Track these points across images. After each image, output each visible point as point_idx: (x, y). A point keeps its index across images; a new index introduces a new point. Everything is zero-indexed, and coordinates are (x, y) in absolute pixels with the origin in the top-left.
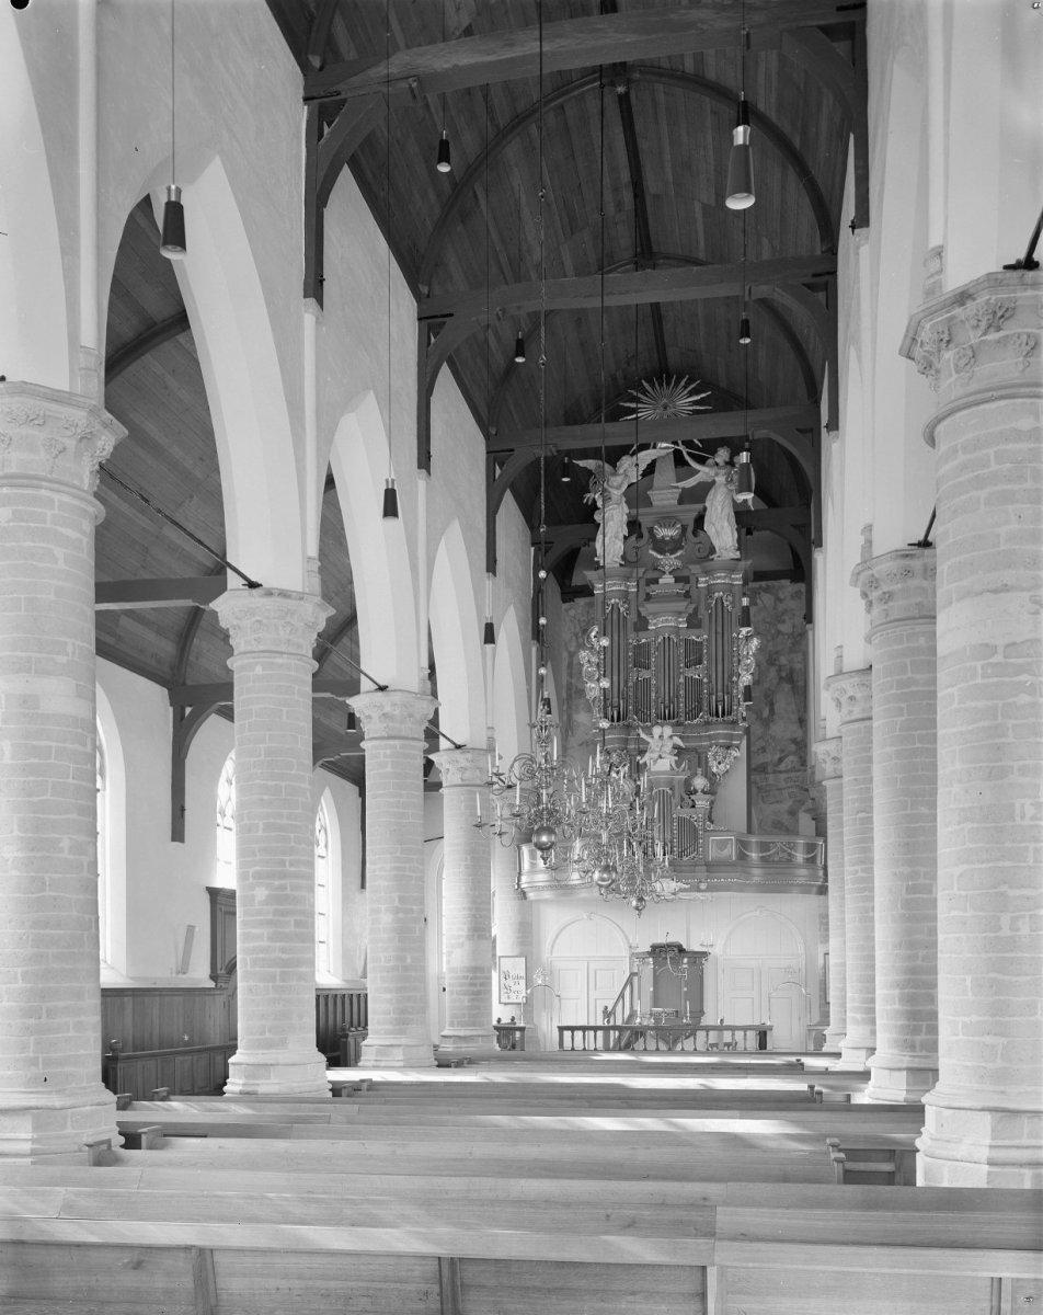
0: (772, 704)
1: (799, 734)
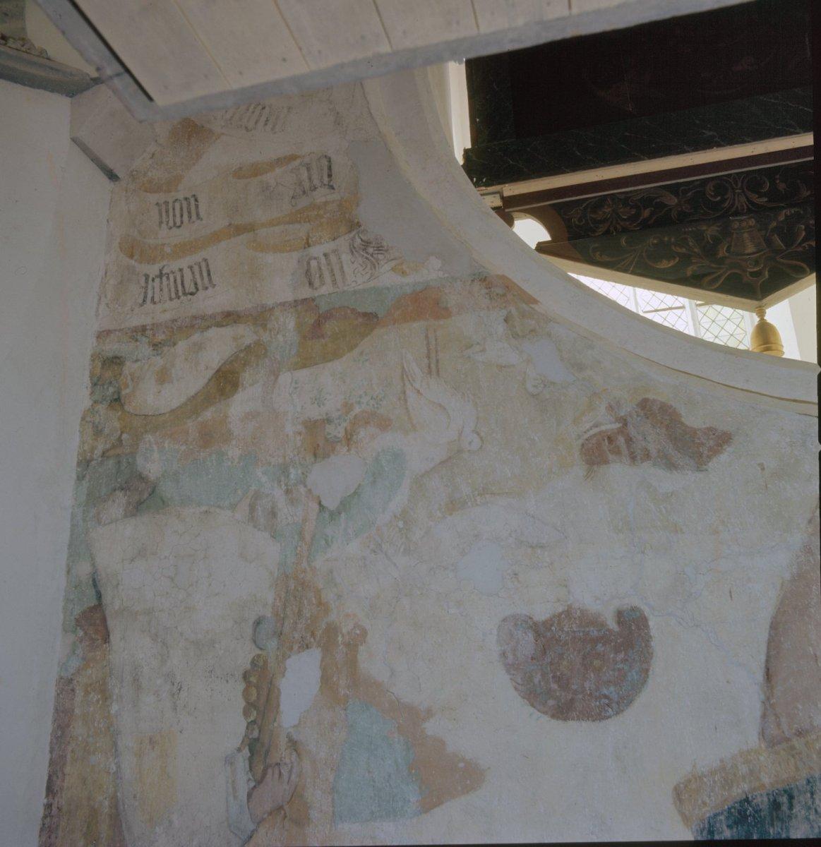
0: (258, 748)
1: (117, 540)
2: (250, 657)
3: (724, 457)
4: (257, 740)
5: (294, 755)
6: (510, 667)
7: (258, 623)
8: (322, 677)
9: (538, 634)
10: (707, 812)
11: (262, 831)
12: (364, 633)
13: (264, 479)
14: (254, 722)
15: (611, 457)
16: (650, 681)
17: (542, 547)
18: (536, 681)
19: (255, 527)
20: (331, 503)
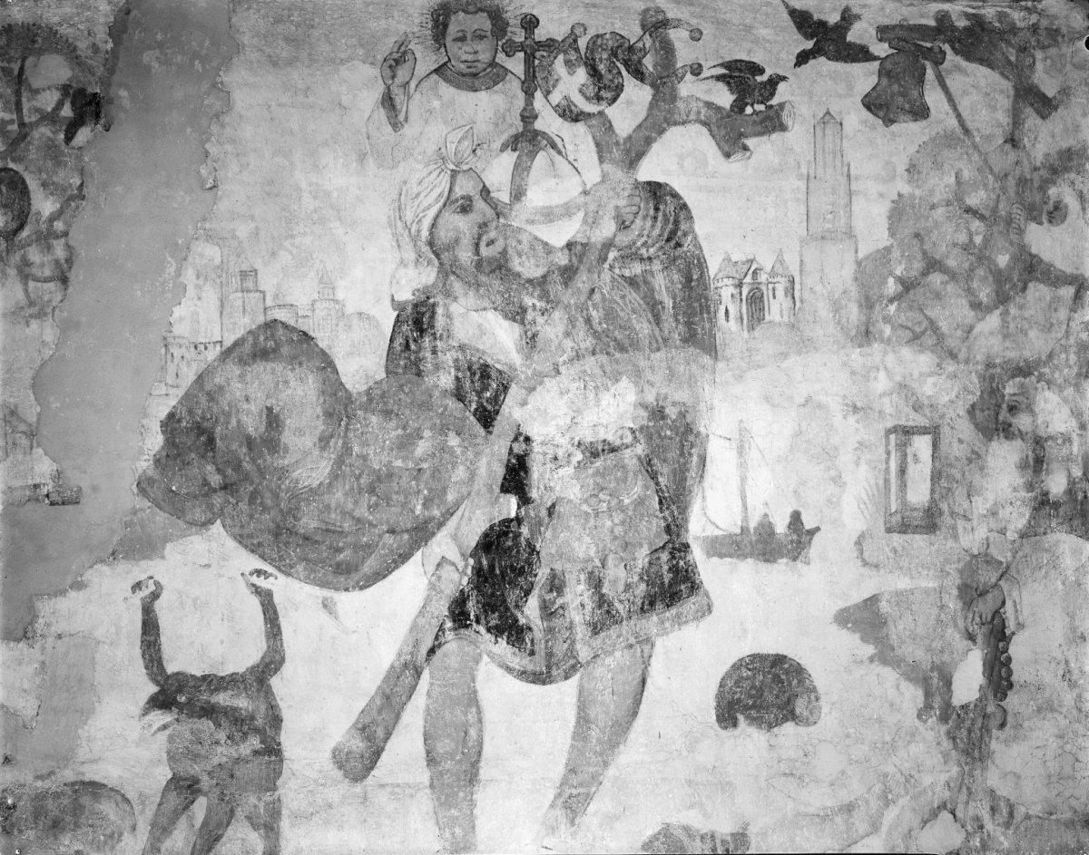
0: (998, 636)
2: (1008, 700)
3: (650, 832)
4: (1000, 640)
5: (970, 630)
6: (814, 690)
7: (1002, 725)
8: (951, 684)
9: (792, 712)
10: (693, 599)
11: (993, 580)
12: (919, 716)
13: (1002, 839)
14: (1003, 653)
15: (729, 838)
16: (719, 680)
17: (785, 774)
18: (795, 681)
19: (1009, 800)
20: (945, 816)
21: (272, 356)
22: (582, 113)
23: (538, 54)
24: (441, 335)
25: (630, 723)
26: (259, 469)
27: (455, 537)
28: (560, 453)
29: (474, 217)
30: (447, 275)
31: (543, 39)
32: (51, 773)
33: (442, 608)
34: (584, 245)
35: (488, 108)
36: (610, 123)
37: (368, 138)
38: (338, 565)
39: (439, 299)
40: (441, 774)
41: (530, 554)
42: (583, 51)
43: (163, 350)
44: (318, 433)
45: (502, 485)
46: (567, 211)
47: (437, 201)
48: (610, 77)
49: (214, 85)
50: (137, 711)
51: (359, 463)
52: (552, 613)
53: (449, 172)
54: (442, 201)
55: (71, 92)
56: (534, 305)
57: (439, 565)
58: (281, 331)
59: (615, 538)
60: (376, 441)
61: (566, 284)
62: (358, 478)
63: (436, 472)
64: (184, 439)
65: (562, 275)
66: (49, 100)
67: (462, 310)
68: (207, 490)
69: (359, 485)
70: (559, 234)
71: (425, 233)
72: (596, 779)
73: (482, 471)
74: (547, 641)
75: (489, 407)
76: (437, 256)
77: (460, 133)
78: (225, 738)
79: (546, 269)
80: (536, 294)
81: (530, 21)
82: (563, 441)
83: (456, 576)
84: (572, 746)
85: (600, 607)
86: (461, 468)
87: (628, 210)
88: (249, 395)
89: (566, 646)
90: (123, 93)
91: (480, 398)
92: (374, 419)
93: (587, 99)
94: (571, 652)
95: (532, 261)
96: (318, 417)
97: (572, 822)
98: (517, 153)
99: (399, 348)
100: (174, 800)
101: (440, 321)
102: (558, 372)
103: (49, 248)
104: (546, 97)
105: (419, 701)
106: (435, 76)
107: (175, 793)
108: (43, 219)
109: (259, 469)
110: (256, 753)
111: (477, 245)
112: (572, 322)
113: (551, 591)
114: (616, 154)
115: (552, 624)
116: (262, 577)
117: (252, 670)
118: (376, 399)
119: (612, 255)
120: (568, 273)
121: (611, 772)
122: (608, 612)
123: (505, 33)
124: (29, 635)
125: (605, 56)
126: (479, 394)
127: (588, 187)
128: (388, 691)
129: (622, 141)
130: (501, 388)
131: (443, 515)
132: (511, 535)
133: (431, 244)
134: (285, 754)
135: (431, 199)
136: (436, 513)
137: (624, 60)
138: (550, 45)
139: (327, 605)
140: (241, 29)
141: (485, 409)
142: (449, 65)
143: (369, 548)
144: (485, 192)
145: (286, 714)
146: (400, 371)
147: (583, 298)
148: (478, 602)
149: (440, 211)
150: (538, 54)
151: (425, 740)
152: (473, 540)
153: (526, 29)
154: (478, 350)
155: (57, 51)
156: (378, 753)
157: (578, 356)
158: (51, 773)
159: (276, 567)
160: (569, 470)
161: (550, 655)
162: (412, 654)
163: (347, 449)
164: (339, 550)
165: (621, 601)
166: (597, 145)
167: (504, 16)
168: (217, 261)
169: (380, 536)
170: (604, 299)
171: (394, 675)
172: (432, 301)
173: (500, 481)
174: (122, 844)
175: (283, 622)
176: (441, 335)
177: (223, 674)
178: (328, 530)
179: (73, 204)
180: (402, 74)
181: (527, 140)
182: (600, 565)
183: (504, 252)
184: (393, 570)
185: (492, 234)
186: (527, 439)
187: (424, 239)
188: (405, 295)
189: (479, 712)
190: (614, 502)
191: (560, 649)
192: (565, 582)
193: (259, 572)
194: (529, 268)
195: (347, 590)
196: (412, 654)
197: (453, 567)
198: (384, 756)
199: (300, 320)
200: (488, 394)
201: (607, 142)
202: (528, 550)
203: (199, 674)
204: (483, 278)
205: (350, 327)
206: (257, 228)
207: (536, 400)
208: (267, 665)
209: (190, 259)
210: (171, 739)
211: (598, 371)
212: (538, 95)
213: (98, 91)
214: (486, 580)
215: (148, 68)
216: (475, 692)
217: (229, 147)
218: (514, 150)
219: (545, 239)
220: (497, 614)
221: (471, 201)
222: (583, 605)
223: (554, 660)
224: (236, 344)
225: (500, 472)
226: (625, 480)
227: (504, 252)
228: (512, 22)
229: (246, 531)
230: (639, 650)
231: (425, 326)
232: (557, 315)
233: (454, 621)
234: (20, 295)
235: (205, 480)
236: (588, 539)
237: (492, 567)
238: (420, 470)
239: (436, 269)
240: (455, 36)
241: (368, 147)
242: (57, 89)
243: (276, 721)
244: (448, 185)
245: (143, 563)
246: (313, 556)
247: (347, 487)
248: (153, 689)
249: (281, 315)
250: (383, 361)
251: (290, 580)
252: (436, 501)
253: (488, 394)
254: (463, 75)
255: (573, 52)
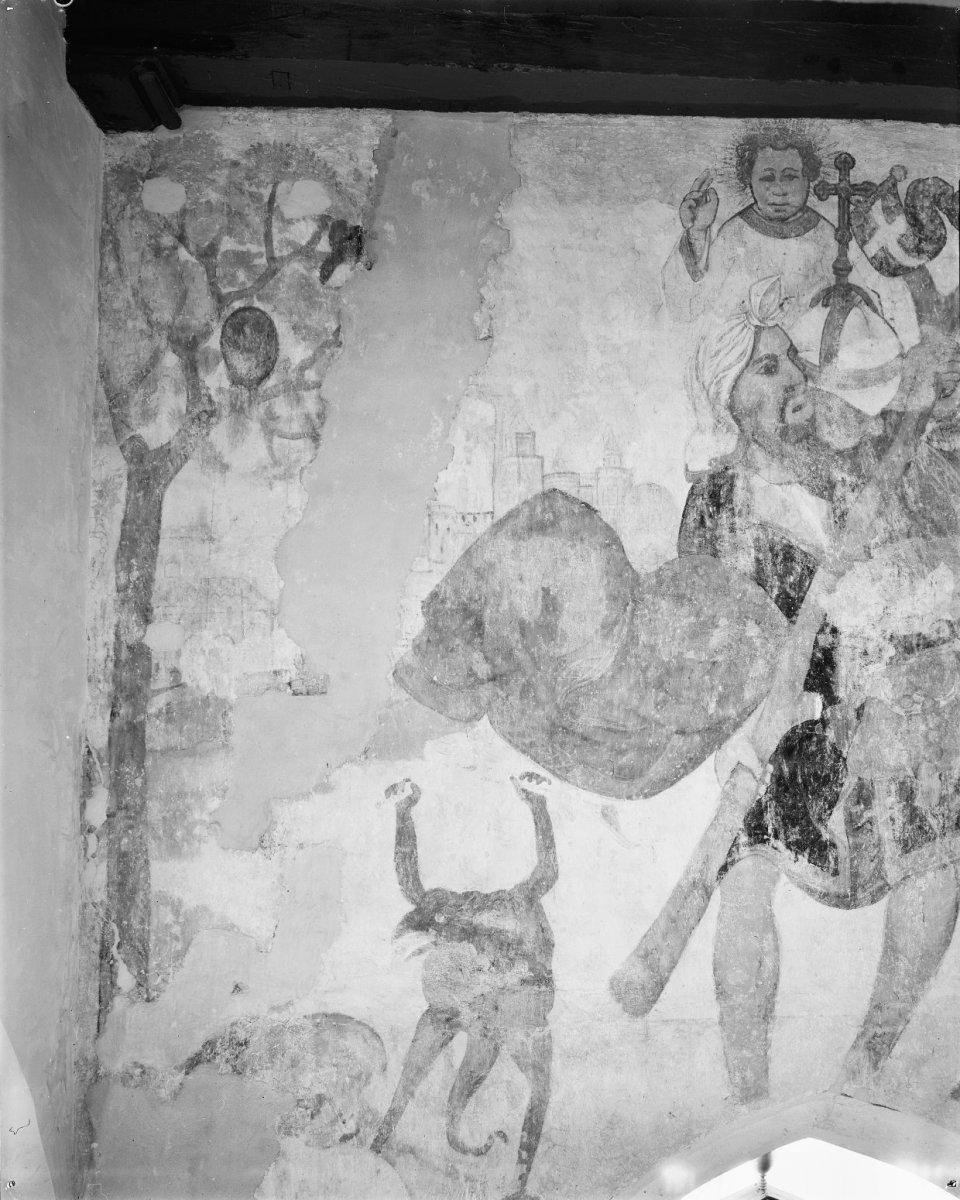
21: (550, 530)
22: (901, 266)
23: (854, 199)
24: (740, 512)
25: (941, 954)
26: (533, 659)
27: (752, 741)
28: (871, 647)
29: (780, 379)
30: (748, 443)
31: (859, 182)
32: (289, 1003)
33: (737, 820)
34: (900, 414)
35: (798, 257)
36: (931, 278)
37: (664, 288)
38: (621, 769)
39: (739, 470)
40: (733, 1009)
41: (836, 761)
42: (903, 197)
43: (426, 521)
44: (600, 618)
45: (806, 683)
46: (882, 375)
47: (739, 360)
48: (932, 227)
49: (492, 223)
50: (390, 932)
51: (646, 654)
52: (859, 828)
53: (753, 328)
54: (743, 363)
55: (330, 224)
56: (843, 480)
57: (734, 771)
58: (560, 502)
59: (930, 744)
60: (667, 628)
61: (879, 458)
62: (644, 671)
63: (732, 665)
64: (449, 622)
65: (875, 447)
66: (303, 232)
67: (763, 483)
68: (473, 680)
69: (645, 678)
70: (874, 401)
71: (725, 396)
72: (903, 1017)
73: (784, 665)
74: (852, 860)
75: (793, 594)
76: (738, 421)
77: (766, 285)
78: (489, 964)
79: (857, 440)
80: (846, 468)
81: (845, 161)
82: (875, 634)
83: (753, 784)
84: (878, 980)
85: (911, 821)
86: (761, 662)
87: (949, 376)
88: (522, 576)
89: (873, 865)
90: (389, 227)
91: (782, 583)
92: (664, 604)
93: (907, 251)
94: (879, 873)
95: (843, 430)
96: (601, 600)
97: (875, 1066)
98: (828, 309)
99: (693, 525)
100: (431, 1035)
101: (739, 495)
102: (870, 556)
103: (299, 400)
104: (861, 247)
105: (709, 926)
106: (739, 220)
107: (431, 1027)
108: (293, 367)
109: (533, 659)
110: (524, 981)
111: (782, 410)
112: (885, 499)
113: (858, 803)
114: (937, 314)
115: (858, 840)
116: (534, 782)
117: (521, 887)
118: (671, 584)
119: (930, 426)
120: (882, 445)
121: (920, 1008)
122: (920, 828)
123: (817, 174)
124: (265, 844)
125: (927, 204)
126: (782, 578)
127: (907, 349)
128: (674, 914)
129: (943, 300)
130: (806, 572)
131: (739, 715)
132: (815, 739)
133: (731, 408)
134: (556, 983)
135: (732, 357)
136: (732, 712)
137: (947, 209)
138: (867, 189)
139: (606, 815)
140: (523, 159)
141: (788, 596)
142: (755, 207)
143: (656, 751)
144: (793, 351)
145: (558, 937)
146: (695, 550)
147: (898, 473)
148: (776, 813)
149: (742, 372)
150: (854, 199)
151: (715, 970)
152: (772, 744)
153: (840, 170)
154: (780, 529)
155: (315, 177)
156: (661, 985)
157: (892, 539)
158: (289, 1003)
159: (550, 770)
160: (881, 667)
161: (855, 875)
162: (701, 871)
163: (633, 638)
164: (622, 752)
165: (934, 816)
166: (917, 303)
167: (817, 153)
168: (490, 421)
169: (668, 738)
170: (920, 476)
171: (681, 895)
172: (730, 472)
173: (803, 677)
174: (371, 1086)
175: (557, 832)
176: (740, 512)
177: (488, 892)
178: (609, 730)
179: (328, 351)
180: (704, 216)
181: (840, 294)
182: (912, 774)
183: (812, 420)
184: (682, 777)
185: (800, 399)
186: (834, 631)
187: (723, 403)
188: (702, 465)
189: (776, 939)
190: (929, 704)
191: (866, 869)
192: (873, 794)
193: (530, 776)
194: (839, 438)
195: (629, 797)
196: (701, 871)
197: (749, 775)
198: (668, 987)
199: (583, 490)
200: (792, 579)
201: (927, 301)
202: (834, 756)
203: (460, 891)
204: (788, 448)
205: (638, 499)
206: (537, 386)
207: (845, 587)
208: (537, 882)
209: (460, 417)
210: (427, 966)
211: (913, 556)
212: (853, 244)
213: (360, 224)
214: (786, 789)
215: (417, 201)
216: (772, 916)
217: (507, 293)
218: (825, 305)
219: (858, 407)
220: (798, 828)
221: (776, 361)
222: (892, 819)
223: (860, 881)
224: (510, 515)
225: (804, 667)
226: (941, 680)
227: (812, 420)
228: (825, 161)
229: (519, 729)
230: (953, 871)
231: (722, 501)
232: (870, 491)
233: (750, 835)
234: (263, 452)
235: (471, 670)
236: (899, 745)
237: (793, 775)
238: (714, 663)
239: (736, 437)
240: (762, 175)
241: (663, 299)
242: (314, 220)
243: (547, 945)
244: (753, 339)
245: (400, 764)
246: (592, 758)
247: (632, 681)
248: (409, 908)
249: (562, 484)
250: (675, 539)
251: (565, 785)
252: (732, 699)
253: (792, 579)
254: (771, 220)
255: (892, 198)
